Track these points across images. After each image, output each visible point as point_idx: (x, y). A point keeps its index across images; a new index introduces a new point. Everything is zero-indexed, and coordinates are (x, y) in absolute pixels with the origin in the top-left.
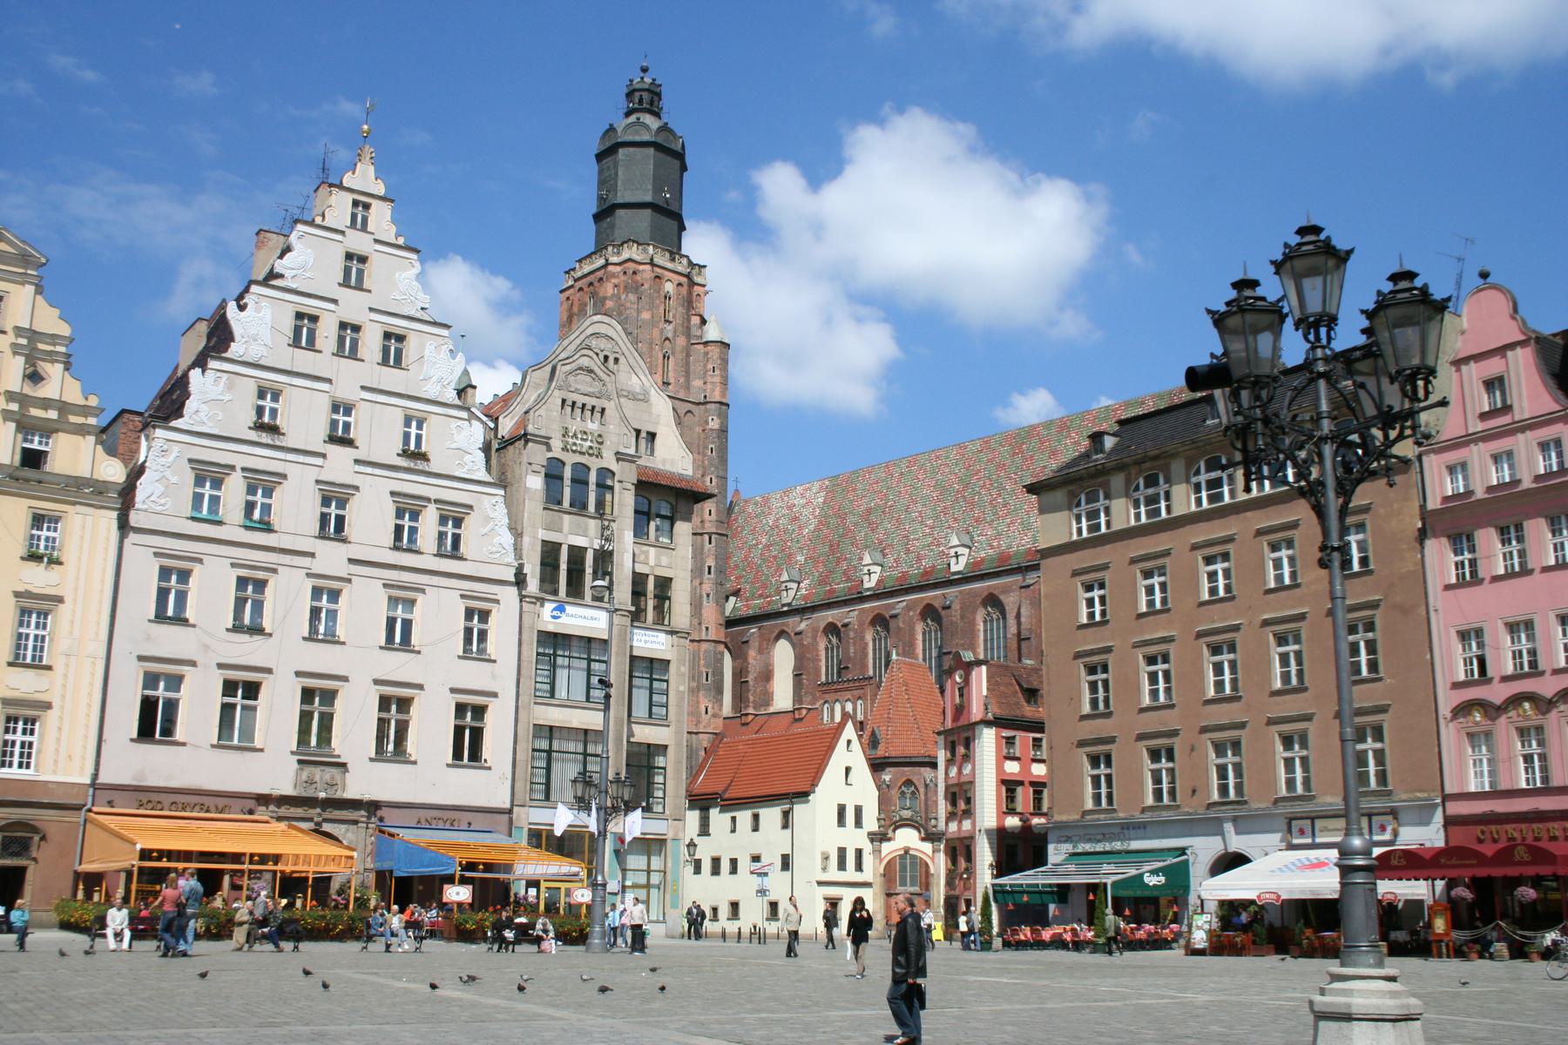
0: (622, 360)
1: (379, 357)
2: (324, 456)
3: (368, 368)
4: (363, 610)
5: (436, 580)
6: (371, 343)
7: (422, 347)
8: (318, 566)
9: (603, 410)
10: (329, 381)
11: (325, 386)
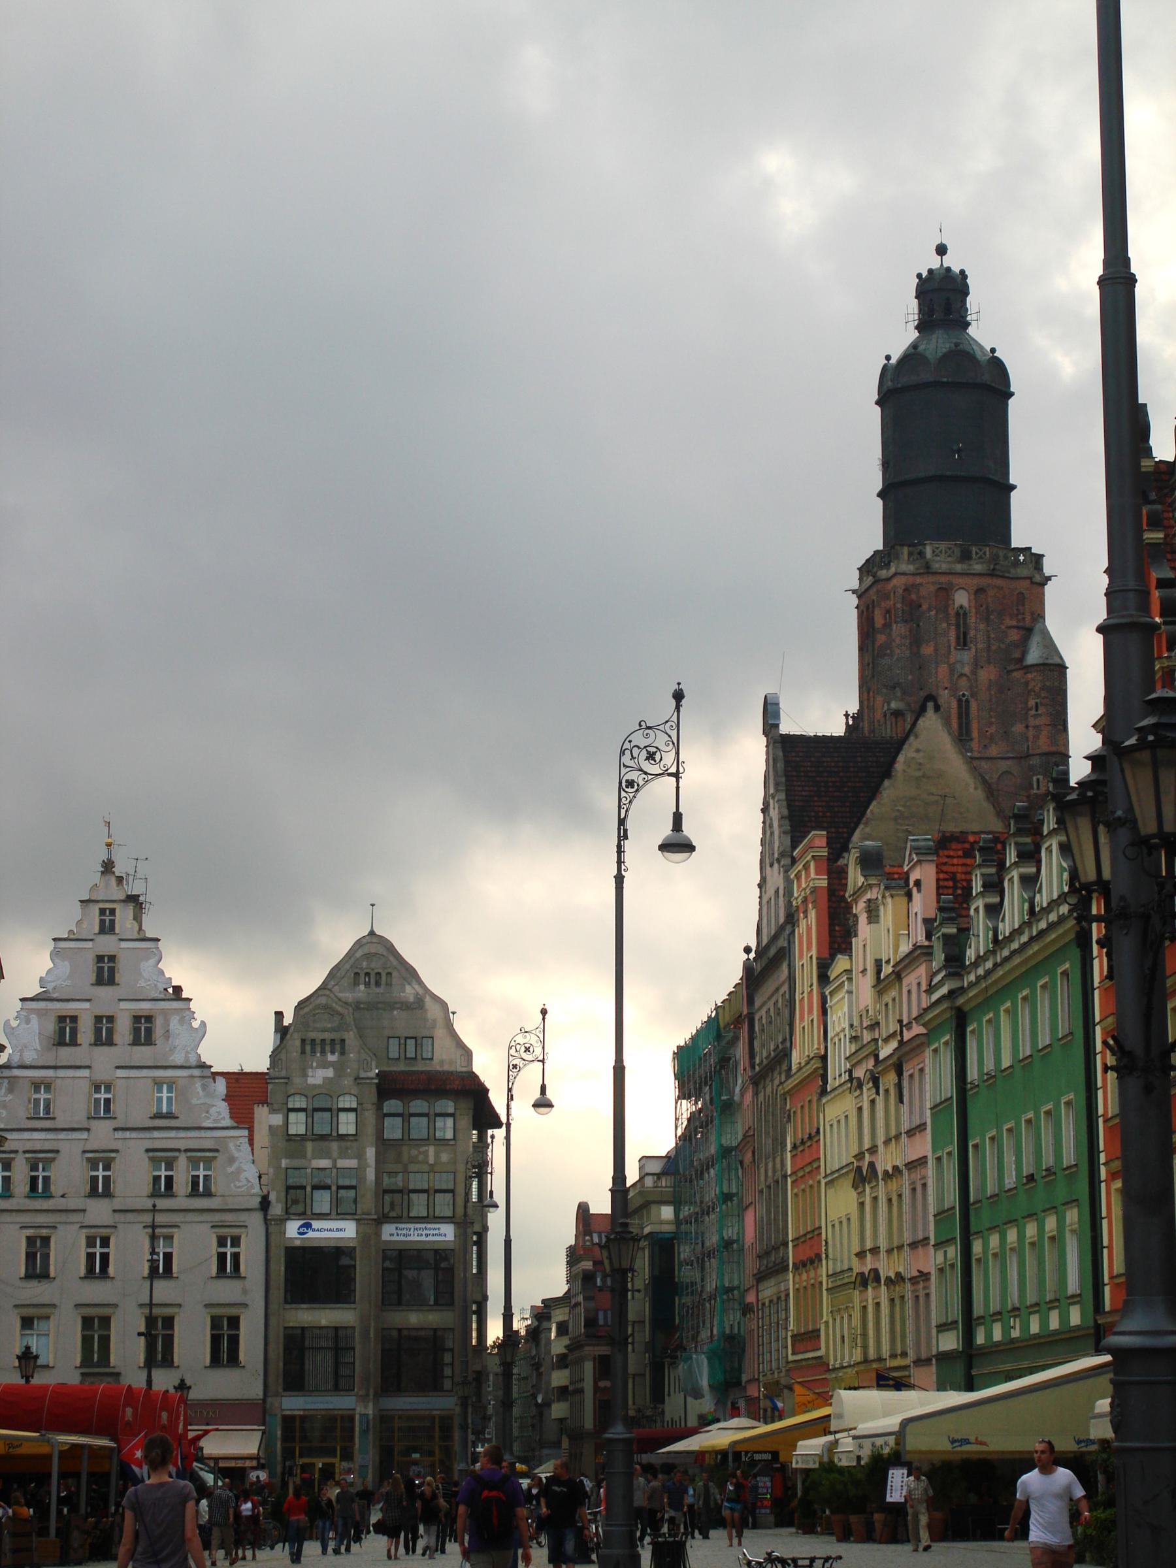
0: (395, 974)
1: (129, 1038)
2: (88, 1130)
3: (122, 1050)
4: (130, 1251)
5: (190, 1217)
6: (123, 1029)
7: (167, 1023)
8: (90, 1219)
9: (343, 1041)
10: (88, 1067)
11: (85, 1073)
